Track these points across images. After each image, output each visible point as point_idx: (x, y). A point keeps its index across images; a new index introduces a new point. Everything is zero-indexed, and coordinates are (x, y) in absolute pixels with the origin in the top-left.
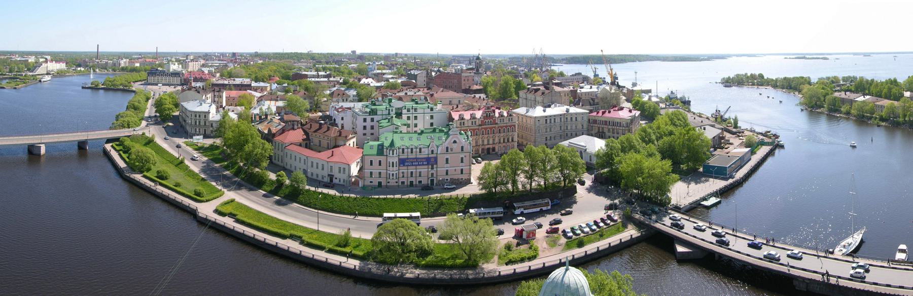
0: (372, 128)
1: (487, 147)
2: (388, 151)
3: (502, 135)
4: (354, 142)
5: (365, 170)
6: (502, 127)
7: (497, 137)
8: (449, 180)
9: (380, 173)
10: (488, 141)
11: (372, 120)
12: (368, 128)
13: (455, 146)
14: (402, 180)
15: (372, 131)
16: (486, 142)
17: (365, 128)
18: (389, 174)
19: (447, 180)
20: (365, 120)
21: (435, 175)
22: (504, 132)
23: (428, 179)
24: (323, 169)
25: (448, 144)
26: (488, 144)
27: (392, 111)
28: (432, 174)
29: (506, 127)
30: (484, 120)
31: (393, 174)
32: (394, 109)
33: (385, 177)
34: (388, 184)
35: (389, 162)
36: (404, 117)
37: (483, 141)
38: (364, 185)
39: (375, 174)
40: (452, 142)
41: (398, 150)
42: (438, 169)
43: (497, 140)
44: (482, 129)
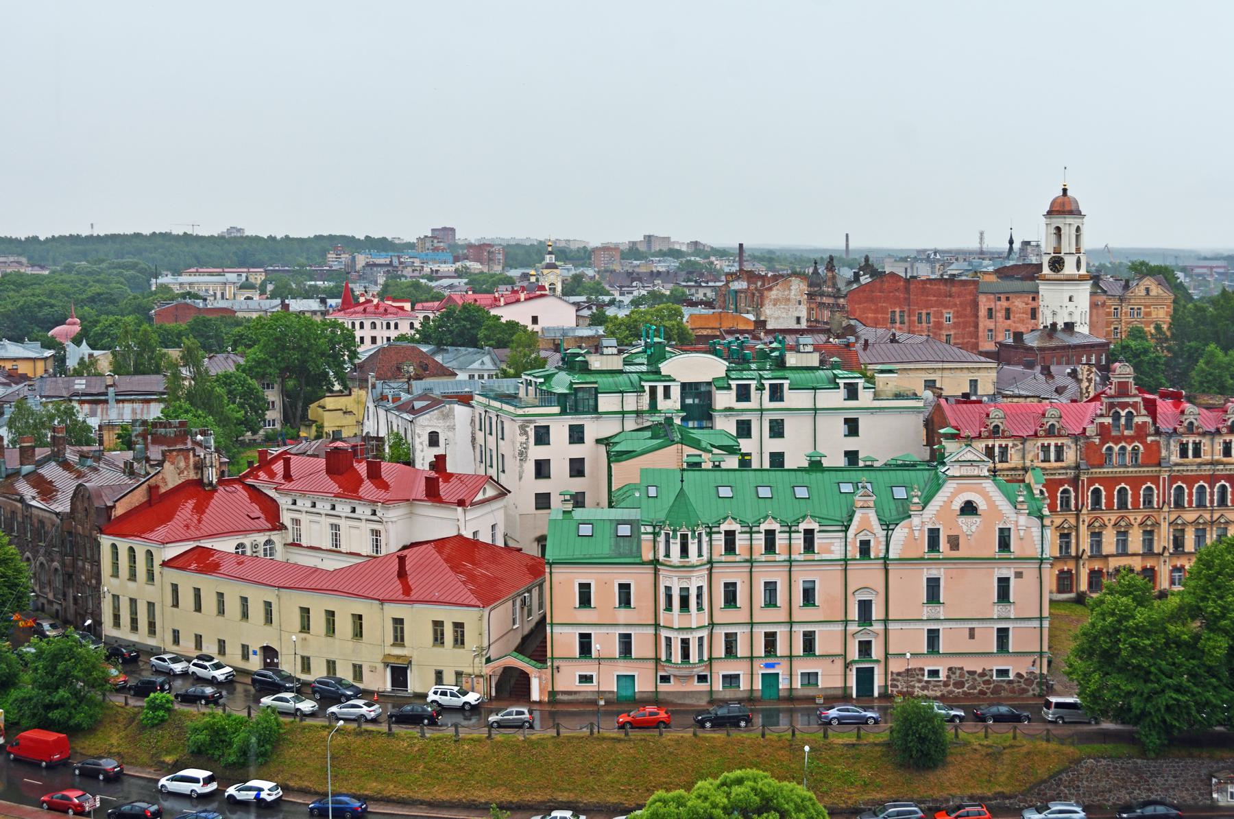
0: (577, 468)
1: (1114, 563)
2: (662, 539)
3: (1190, 516)
4: (493, 527)
5: (557, 630)
6: (1190, 481)
7: (1164, 526)
8: (942, 676)
9: (626, 641)
10: (1123, 535)
11: (577, 435)
12: (560, 469)
13: (967, 525)
14: (723, 668)
15: (577, 485)
16: (1109, 543)
17: (542, 469)
18: (668, 640)
19: (934, 673)
20: (542, 436)
21: (877, 652)
22: (1201, 505)
23: (847, 666)
24: (358, 633)
25: (938, 515)
26: (1124, 553)
27: (667, 395)
28: (865, 647)
29: (1212, 480)
30: (1103, 442)
31: (685, 643)
32: (676, 391)
33: (652, 655)
34: (663, 687)
35: (668, 589)
36: (726, 425)
37: (1096, 536)
38: (553, 693)
39: (605, 643)
40: (957, 504)
41: (705, 539)
42: (891, 626)
43: (1164, 538)
44: (1091, 481)
